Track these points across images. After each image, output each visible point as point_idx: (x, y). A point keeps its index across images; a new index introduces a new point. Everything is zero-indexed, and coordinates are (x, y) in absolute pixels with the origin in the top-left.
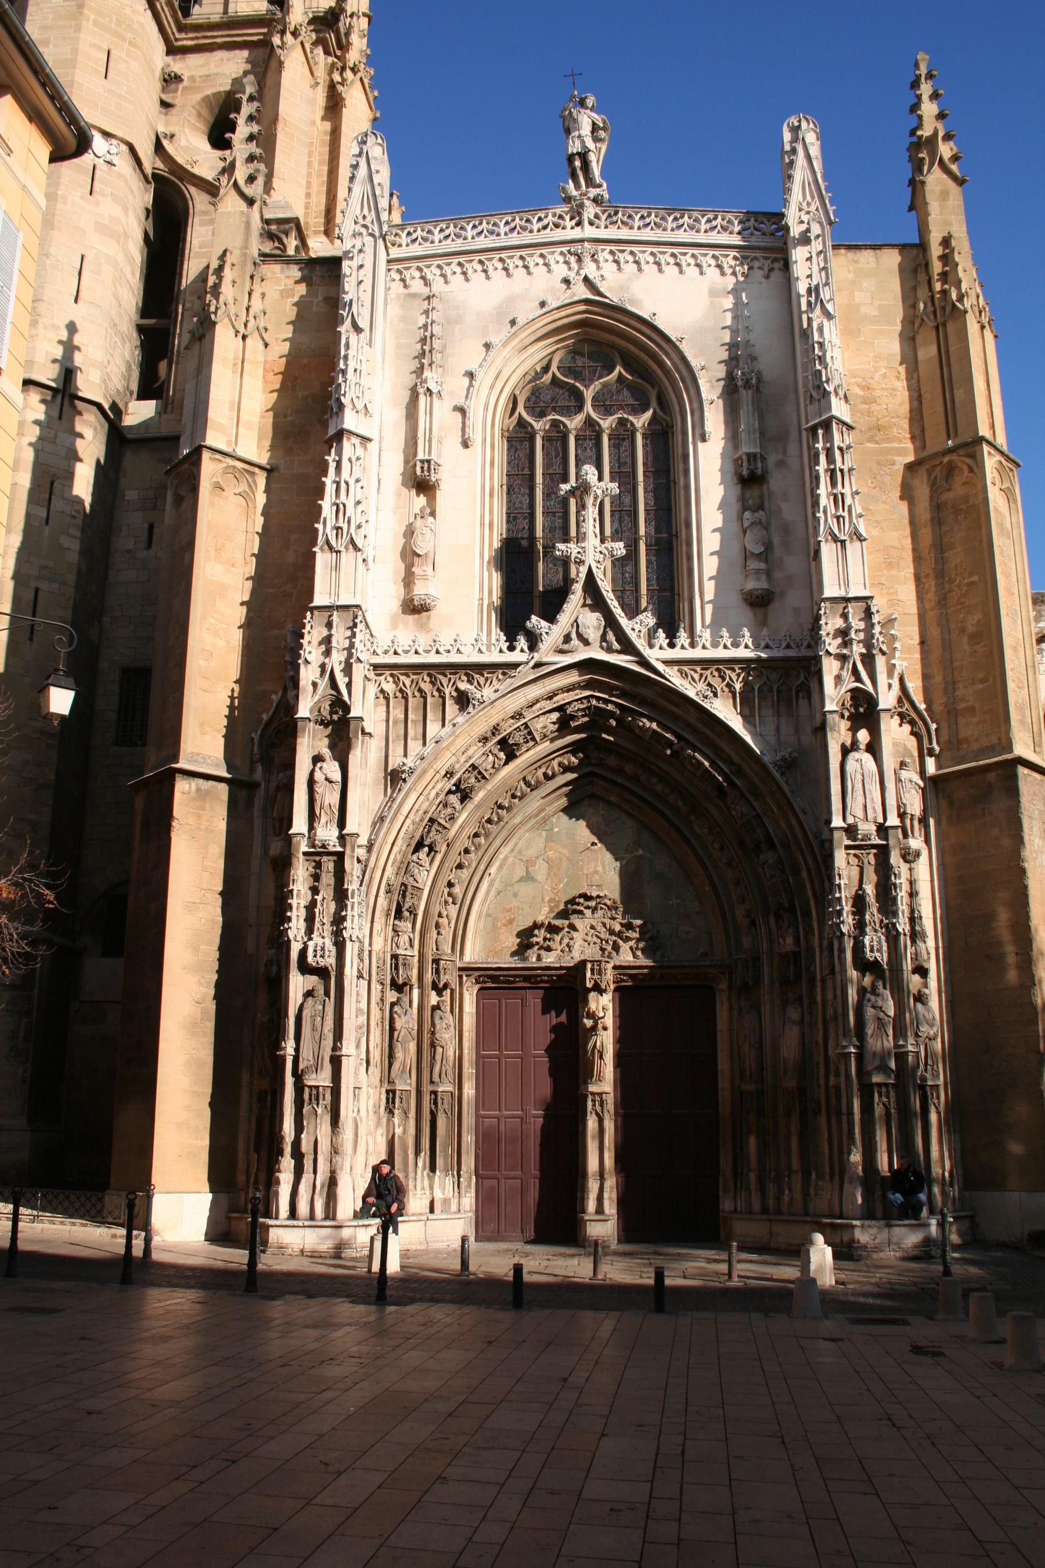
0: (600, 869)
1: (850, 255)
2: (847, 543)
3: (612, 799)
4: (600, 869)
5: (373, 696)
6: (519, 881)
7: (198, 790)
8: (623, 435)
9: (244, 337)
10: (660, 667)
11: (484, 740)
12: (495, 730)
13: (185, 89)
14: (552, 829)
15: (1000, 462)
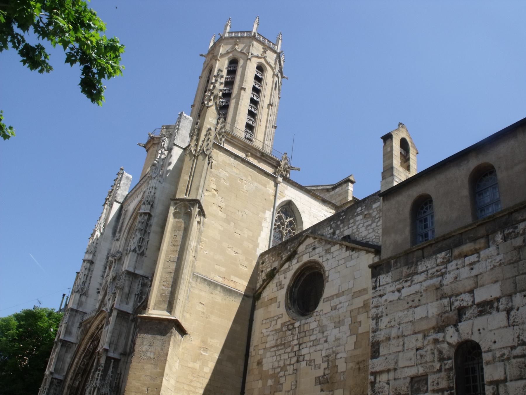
11: (90, 339)
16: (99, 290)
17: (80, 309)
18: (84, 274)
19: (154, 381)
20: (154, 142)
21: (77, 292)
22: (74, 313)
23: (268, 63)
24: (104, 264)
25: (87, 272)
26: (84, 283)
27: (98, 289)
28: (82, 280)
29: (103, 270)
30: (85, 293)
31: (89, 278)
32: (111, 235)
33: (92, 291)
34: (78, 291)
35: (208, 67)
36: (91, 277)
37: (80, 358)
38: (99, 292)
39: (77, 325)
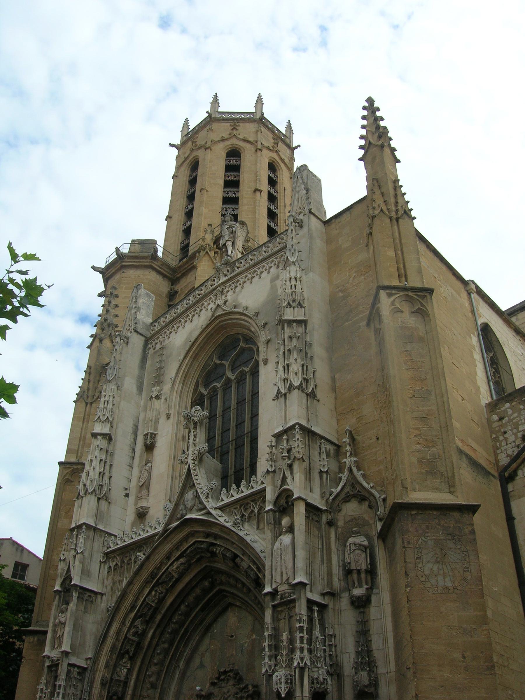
0: (234, 652)
1: (337, 221)
2: (287, 395)
3: (238, 604)
4: (234, 652)
5: (106, 572)
6: (197, 669)
7: (38, 640)
8: (240, 380)
9: (91, 403)
10: (213, 512)
11: (147, 582)
12: (153, 575)
13: (180, 294)
14: (213, 631)
15: (407, 295)
16: (127, 492)
17: (100, 527)
18: (99, 459)
19: (472, 636)
20: (123, 264)
21: (92, 493)
22: (92, 534)
23: (282, 160)
24: (130, 443)
25: (103, 457)
26: (101, 474)
27: (126, 489)
28: (97, 470)
29: (131, 455)
30: (105, 495)
31: (107, 467)
32: (135, 390)
33: (117, 494)
34: (94, 490)
35: (188, 161)
36: (111, 466)
37: (123, 623)
38: (127, 495)
39: (98, 557)
